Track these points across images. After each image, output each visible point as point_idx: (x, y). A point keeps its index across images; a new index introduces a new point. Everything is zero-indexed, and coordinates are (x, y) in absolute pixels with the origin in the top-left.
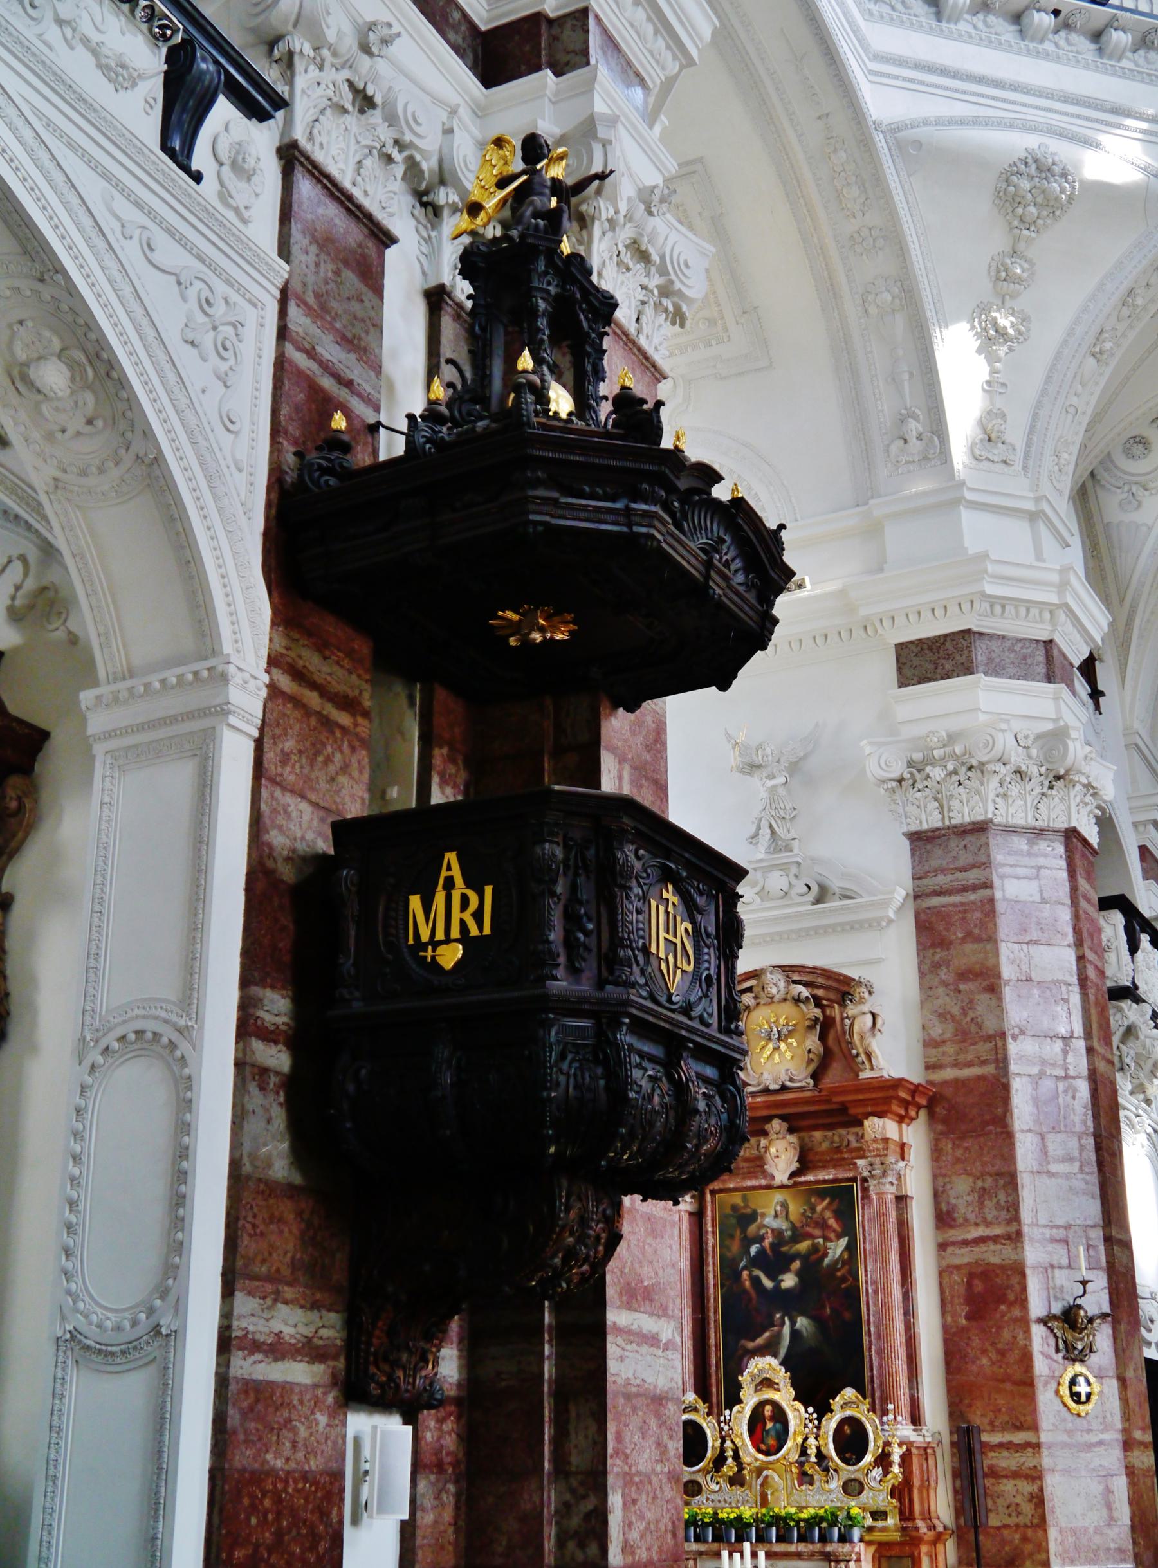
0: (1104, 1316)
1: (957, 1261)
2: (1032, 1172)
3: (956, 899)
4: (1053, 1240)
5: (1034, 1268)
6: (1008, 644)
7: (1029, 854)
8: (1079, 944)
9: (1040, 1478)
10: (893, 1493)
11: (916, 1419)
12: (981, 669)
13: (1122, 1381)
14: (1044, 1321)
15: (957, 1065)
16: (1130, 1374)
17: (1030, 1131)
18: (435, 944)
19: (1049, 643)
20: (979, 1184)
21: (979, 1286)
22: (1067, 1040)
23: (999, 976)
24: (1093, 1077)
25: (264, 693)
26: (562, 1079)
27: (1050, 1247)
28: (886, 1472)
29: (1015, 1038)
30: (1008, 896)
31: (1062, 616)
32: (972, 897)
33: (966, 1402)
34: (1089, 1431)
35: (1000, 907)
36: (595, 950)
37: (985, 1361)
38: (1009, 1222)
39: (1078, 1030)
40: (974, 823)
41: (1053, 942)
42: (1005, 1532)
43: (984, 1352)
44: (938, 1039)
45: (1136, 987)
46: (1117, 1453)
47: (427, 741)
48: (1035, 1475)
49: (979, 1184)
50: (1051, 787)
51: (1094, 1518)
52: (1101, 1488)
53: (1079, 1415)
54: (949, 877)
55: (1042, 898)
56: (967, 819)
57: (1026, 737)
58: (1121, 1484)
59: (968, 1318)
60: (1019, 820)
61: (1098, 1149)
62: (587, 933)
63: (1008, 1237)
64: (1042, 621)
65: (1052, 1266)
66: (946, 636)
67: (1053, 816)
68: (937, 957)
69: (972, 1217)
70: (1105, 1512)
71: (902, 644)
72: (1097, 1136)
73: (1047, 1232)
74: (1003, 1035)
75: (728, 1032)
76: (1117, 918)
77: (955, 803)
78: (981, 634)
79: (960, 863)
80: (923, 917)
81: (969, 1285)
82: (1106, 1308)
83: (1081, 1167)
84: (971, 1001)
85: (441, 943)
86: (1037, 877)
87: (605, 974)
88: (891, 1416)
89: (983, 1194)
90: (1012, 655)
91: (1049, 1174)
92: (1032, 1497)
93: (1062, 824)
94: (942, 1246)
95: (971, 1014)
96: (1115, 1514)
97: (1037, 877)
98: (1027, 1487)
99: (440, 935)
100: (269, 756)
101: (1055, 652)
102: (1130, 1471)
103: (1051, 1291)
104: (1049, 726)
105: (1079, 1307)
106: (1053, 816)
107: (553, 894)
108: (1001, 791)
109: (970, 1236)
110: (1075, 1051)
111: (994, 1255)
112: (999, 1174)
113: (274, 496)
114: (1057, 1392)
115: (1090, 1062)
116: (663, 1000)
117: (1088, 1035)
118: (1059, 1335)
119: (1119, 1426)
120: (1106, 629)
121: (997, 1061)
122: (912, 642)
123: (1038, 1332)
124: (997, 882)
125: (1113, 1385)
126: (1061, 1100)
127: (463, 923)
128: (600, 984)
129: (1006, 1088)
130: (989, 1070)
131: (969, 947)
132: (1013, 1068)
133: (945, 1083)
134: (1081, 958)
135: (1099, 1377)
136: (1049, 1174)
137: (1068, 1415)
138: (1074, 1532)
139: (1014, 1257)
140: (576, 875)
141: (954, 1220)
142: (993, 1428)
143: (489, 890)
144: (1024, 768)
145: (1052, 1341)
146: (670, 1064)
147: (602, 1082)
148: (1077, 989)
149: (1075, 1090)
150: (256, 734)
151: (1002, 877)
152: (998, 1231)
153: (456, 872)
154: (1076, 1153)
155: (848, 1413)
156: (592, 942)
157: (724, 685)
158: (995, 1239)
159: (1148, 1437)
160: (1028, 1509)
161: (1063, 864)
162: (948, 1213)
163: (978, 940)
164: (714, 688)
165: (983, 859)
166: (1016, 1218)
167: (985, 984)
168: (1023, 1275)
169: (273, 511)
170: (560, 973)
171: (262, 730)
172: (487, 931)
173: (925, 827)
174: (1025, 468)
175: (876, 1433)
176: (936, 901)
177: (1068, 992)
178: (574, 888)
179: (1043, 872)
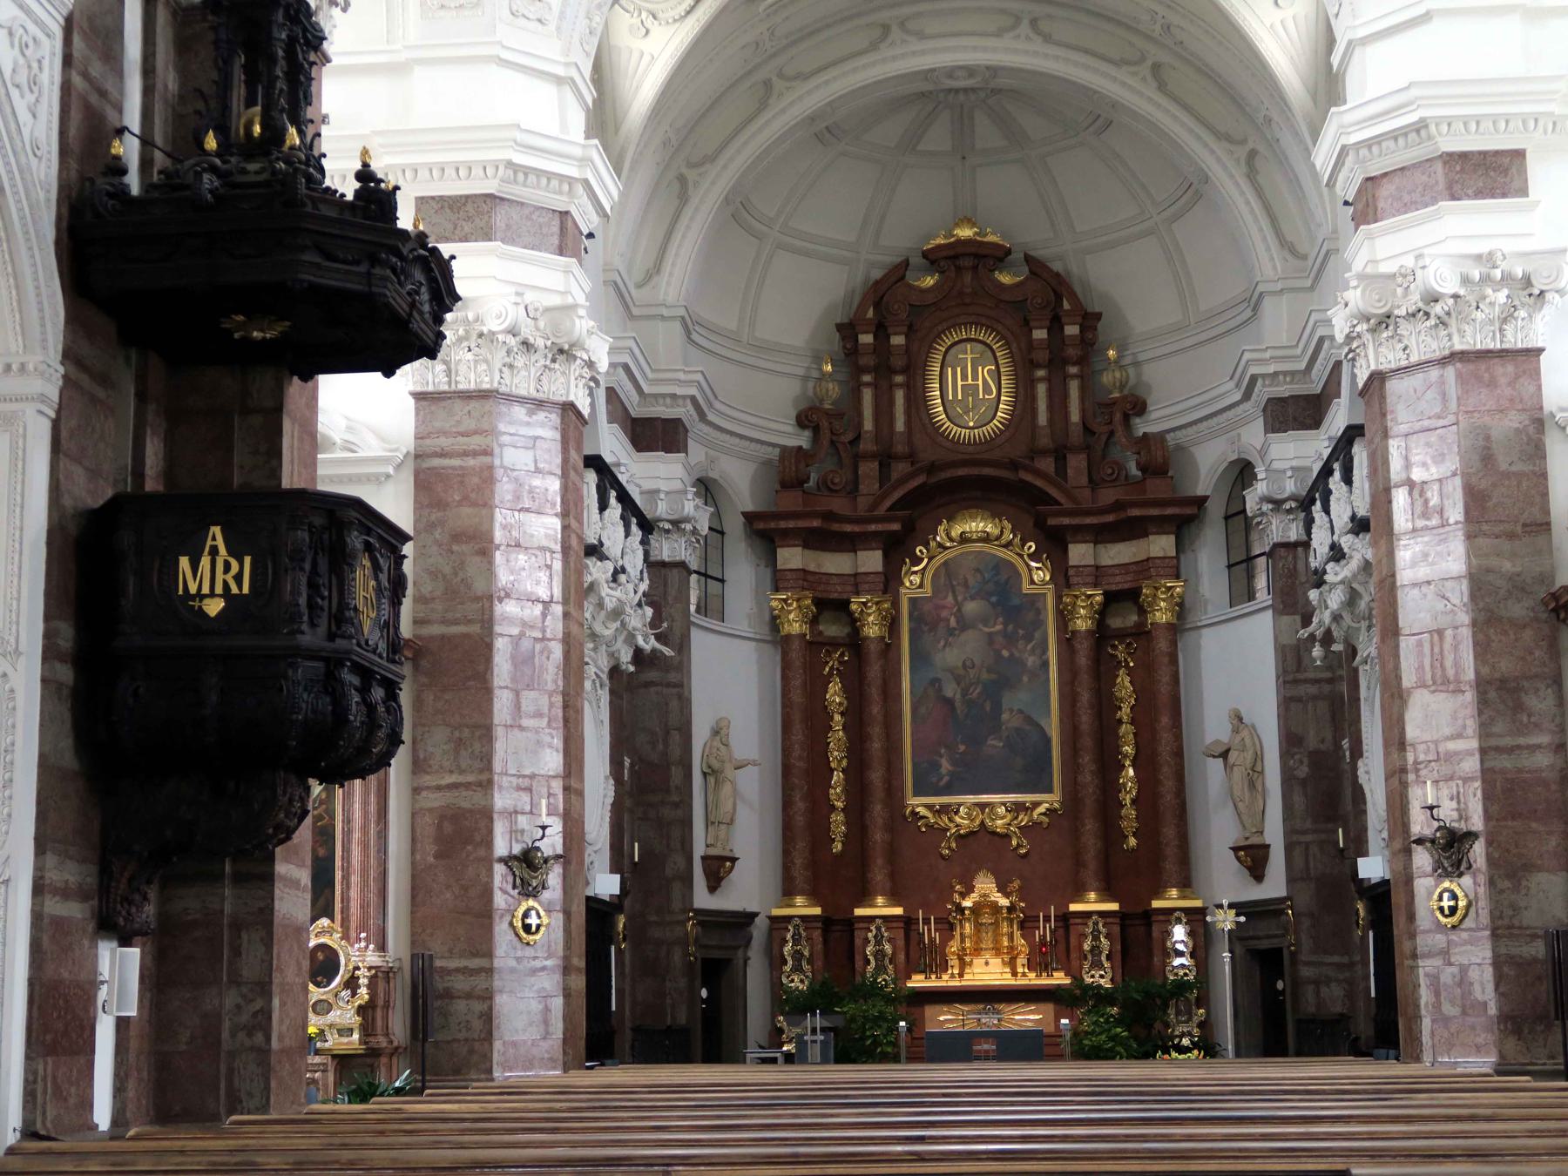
0: (557, 857)
1: (429, 805)
2: (505, 726)
3: (456, 462)
4: (519, 788)
5: (500, 813)
6: (526, 211)
7: (528, 424)
8: (565, 515)
9: (491, 998)
10: (361, 1010)
11: (382, 947)
12: (499, 235)
13: (567, 913)
14: (504, 861)
15: (444, 622)
16: (574, 908)
17: (506, 687)
18: (202, 597)
19: (565, 215)
20: (457, 734)
21: (448, 828)
22: (546, 604)
23: (492, 541)
24: (567, 640)
25: (60, 383)
26: (304, 706)
27: (516, 795)
28: (354, 994)
29: (501, 600)
30: (505, 464)
31: (580, 189)
32: (471, 462)
33: (428, 931)
34: (535, 958)
35: (499, 473)
36: (326, 609)
37: (448, 895)
38: (481, 771)
39: (557, 593)
40: (480, 391)
41: (542, 510)
42: (455, 1045)
43: (448, 887)
44: (428, 596)
45: (601, 544)
46: (558, 977)
47: (141, 397)
48: (488, 996)
49: (457, 734)
50: (554, 361)
51: (534, 1033)
52: (541, 1007)
53: (528, 944)
54: (451, 441)
55: (536, 468)
56: (473, 386)
57: (536, 310)
58: (558, 1003)
59: (436, 857)
60: (523, 392)
61: (566, 707)
62: (323, 598)
63: (480, 784)
64: (561, 193)
65: (516, 812)
66: (467, 197)
67: (553, 389)
68: (433, 517)
69: (446, 764)
70: (542, 1028)
71: (422, 198)
72: (565, 694)
73: (514, 780)
74: (490, 598)
75: (393, 662)
76: (591, 477)
77: (463, 369)
78: (502, 199)
79: (461, 429)
80: (422, 476)
81: (440, 827)
82: (560, 851)
83: (549, 722)
84: (462, 563)
85: (206, 596)
86: (534, 447)
87: (334, 628)
88: (363, 944)
89: (459, 743)
90: (529, 223)
91: (521, 728)
92: (481, 1015)
93: (560, 397)
94: (416, 791)
95: (461, 575)
96: (551, 1029)
97: (534, 447)
98: (478, 1007)
99: (206, 590)
100: (64, 434)
101: (570, 223)
102: (567, 994)
103: (514, 833)
104: (556, 301)
105: (538, 849)
106: (553, 389)
107: (302, 569)
108: (507, 360)
109: (443, 782)
110: (553, 614)
111: (466, 800)
112: (477, 726)
113: (65, 211)
114: (511, 924)
115: (565, 626)
116: (363, 643)
117: (565, 601)
118: (517, 873)
119: (561, 953)
120: (616, 198)
121: (482, 621)
122: (433, 198)
123: (499, 869)
124: (497, 450)
125: (558, 919)
126: (537, 659)
127: (225, 583)
128: (331, 637)
129: (489, 647)
130: (475, 629)
131: (466, 510)
132: (498, 629)
133: (431, 638)
134: (565, 528)
135: (548, 911)
136: (521, 728)
137: (519, 945)
138: (514, 1044)
139: (483, 803)
140: (316, 553)
141: (430, 766)
142: (451, 954)
143: (247, 560)
144: (531, 340)
145: (510, 879)
146: (364, 690)
147: (330, 708)
148: (559, 556)
149: (550, 652)
150: (53, 415)
151: (501, 446)
152: (470, 778)
153: (220, 543)
154: (546, 710)
155: (322, 940)
156: (326, 603)
157: (389, 373)
158: (467, 786)
159: (583, 964)
160: (477, 1024)
161: (558, 436)
162: (425, 760)
163: (474, 504)
164: (379, 374)
165: (486, 426)
166: (488, 766)
167: (476, 547)
168: (491, 820)
169: (64, 224)
170: (305, 627)
171: (59, 412)
172: (246, 590)
173: (430, 388)
174: (558, 29)
175: (348, 961)
176: (436, 462)
177: (552, 559)
178: (314, 564)
179: (538, 443)
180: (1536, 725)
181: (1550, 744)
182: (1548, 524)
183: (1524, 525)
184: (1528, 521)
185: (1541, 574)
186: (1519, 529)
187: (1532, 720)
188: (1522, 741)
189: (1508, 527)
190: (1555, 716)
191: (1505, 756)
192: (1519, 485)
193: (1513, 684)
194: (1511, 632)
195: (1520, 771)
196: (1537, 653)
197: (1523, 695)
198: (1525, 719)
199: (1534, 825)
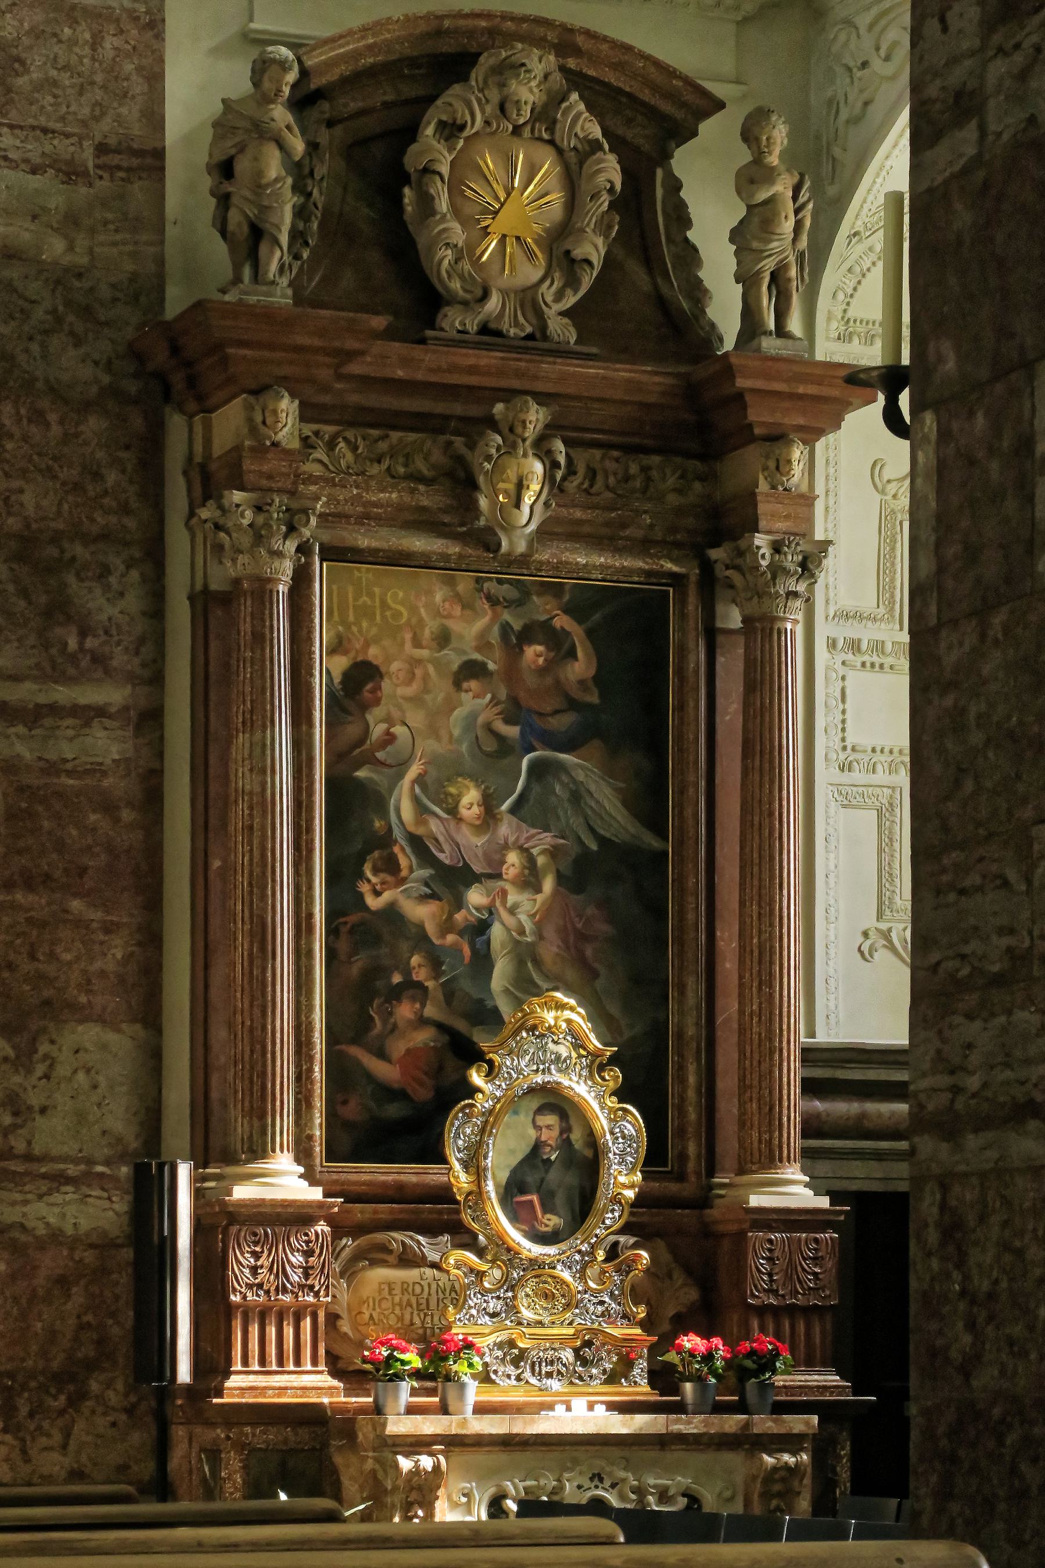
180: (99, 660)
181: (126, 708)
182: (159, 154)
183: (102, 149)
184: (112, 141)
185: (134, 277)
186: (88, 156)
187: (90, 643)
188: (62, 694)
189: (64, 148)
190: (142, 641)
191: (21, 729)
192: (95, 43)
193: (52, 551)
194: (53, 417)
195: (52, 768)
196: (112, 477)
197: (71, 579)
198: (73, 644)
199: (76, 905)
